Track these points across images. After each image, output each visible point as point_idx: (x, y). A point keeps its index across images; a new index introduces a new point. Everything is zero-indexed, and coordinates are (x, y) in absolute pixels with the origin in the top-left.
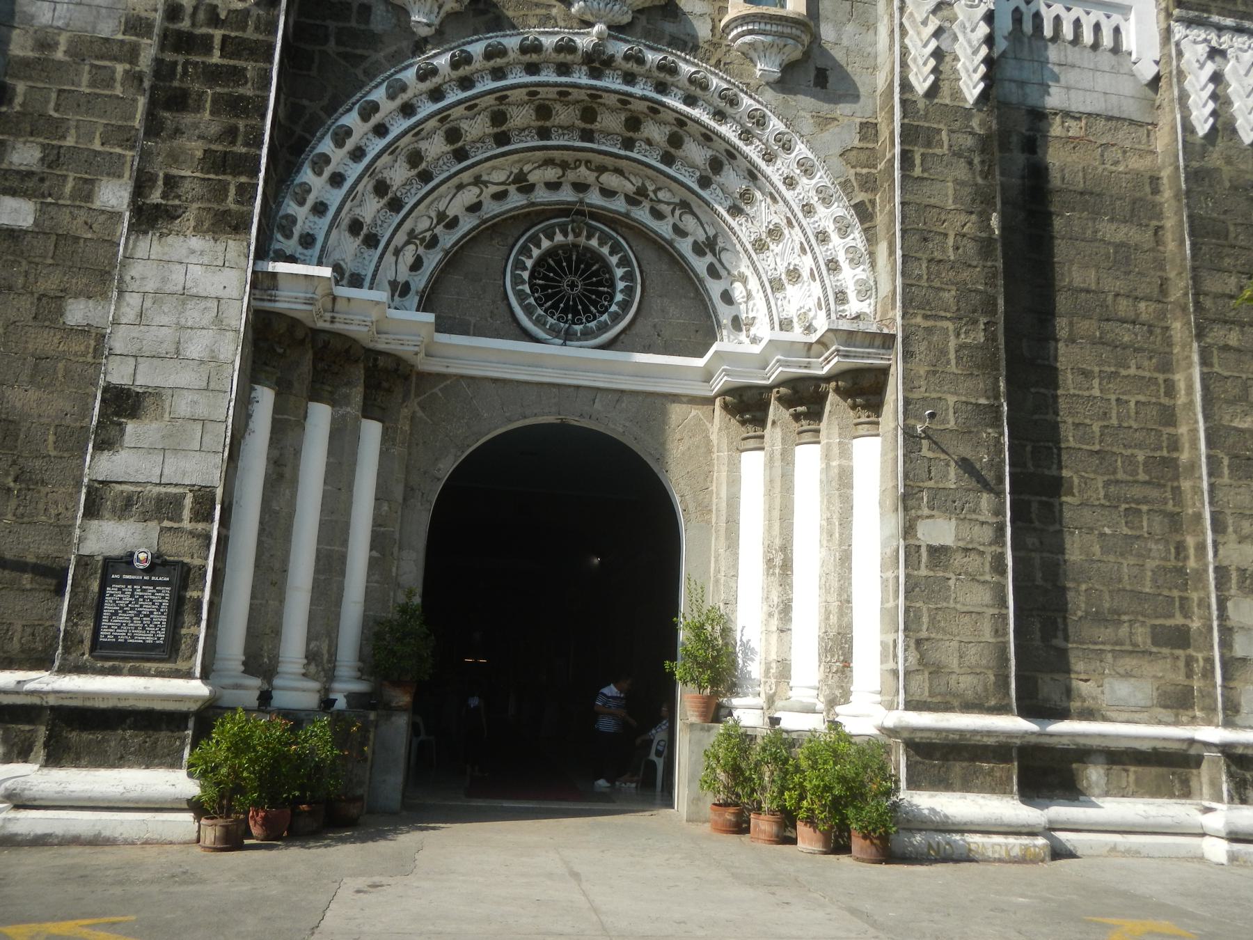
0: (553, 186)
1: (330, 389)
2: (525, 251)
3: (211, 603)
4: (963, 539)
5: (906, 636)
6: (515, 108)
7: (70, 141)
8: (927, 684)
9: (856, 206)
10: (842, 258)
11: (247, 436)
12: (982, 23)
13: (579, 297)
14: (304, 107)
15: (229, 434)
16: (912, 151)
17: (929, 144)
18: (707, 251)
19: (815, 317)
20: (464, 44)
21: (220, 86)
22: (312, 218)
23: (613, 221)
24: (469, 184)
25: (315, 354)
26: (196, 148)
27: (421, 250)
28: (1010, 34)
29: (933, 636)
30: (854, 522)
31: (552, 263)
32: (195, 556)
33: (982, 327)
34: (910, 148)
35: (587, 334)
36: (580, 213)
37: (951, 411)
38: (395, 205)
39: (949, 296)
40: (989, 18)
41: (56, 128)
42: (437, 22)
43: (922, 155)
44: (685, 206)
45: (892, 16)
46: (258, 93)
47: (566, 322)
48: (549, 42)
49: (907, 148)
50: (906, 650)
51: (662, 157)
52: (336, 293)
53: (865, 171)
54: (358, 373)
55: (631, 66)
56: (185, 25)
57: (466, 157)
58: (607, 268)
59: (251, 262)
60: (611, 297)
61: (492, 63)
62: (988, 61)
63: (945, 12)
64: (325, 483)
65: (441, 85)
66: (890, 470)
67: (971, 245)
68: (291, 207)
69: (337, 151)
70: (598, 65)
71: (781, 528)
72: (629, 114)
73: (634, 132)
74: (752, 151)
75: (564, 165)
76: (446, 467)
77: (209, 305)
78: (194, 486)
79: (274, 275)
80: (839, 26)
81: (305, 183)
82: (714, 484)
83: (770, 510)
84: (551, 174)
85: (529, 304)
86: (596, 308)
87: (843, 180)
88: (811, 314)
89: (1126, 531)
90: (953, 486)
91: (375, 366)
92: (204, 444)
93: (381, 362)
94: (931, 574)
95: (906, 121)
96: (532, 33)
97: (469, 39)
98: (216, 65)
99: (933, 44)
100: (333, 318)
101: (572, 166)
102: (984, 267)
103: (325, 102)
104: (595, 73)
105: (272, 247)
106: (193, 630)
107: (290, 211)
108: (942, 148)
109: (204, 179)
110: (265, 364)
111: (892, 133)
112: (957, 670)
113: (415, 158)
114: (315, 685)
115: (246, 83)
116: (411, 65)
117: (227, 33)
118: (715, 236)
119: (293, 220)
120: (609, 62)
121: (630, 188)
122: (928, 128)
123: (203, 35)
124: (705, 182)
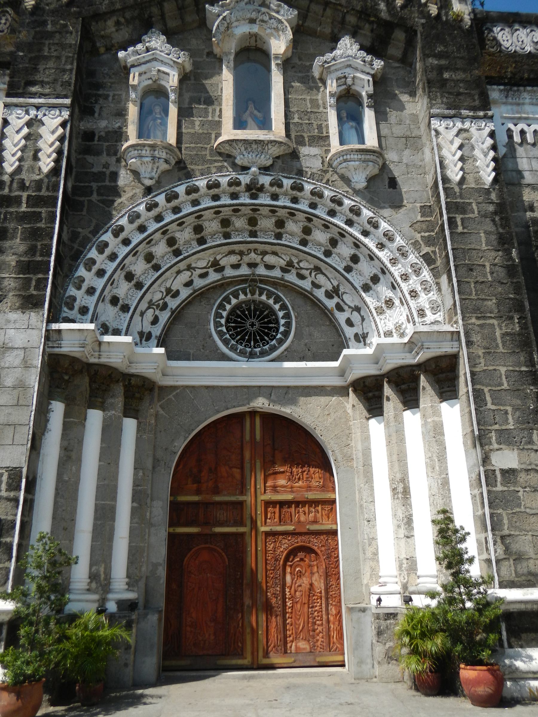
0: (236, 266)
1: (100, 400)
2: (221, 306)
3: (19, 545)
4: (525, 463)
5: (493, 535)
6: (207, 222)
8: (513, 568)
9: (423, 256)
10: (419, 288)
11: (46, 434)
12: (488, 138)
13: (257, 332)
14: (79, 233)
15: (31, 432)
16: (455, 218)
17: (464, 212)
18: (334, 295)
19: (406, 328)
20: (173, 187)
21: (26, 223)
22: (86, 297)
23: (275, 283)
24: (184, 270)
25: (91, 379)
26: (11, 259)
27: (157, 312)
28: (507, 144)
29: (512, 533)
30: (448, 458)
31: (239, 313)
32: (9, 513)
33: (517, 321)
34: (453, 215)
35: (263, 354)
36: (252, 280)
37: (504, 377)
38: (139, 286)
39: (491, 303)
40: (492, 135)
42: (156, 176)
43: (462, 219)
44: (317, 269)
45: (431, 141)
46: (49, 225)
47: (250, 347)
48: (224, 181)
49: (451, 216)
50: (494, 544)
51: (300, 242)
52: (101, 340)
53: (427, 234)
54: (119, 390)
55: (275, 189)
57: (180, 254)
58: (273, 312)
59: (45, 325)
60: (277, 330)
61: (190, 196)
62: (494, 159)
63: (465, 135)
64: (100, 460)
65: (161, 212)
66: (467, 420)
67: (500, 269)
68: (72, 291)
69: (100, 256)
70: (254, 191)
71: (400, 466)
72: (277, 219)
73: (281, 229)
75: (241, 253)
76: (180, 445)
77: (19, 353)
78: (8, 467)
79: (59, 331)
80: (400, 152)
81: (81, 276)
82: (353, 442)
83: (390, 455)
84: (234, 259)
85: (226, 338)
86: (268, 337)
87: (413, 241)
88: (404, 326)
90: (512, 427)
91: (130, 383)
92: (15, 440)
93: (133, 382)
94: (506, 489)
95: (449, 200)
96: (214, 177)
97: (176, 184)
98: (24, 212)
99: (459, 154)
100: (100, 355)
101: (246, 253)
102: (512, 283)
103: (92, 228)
104: (254, 196)
105: (61, 316)
106: (7, 564)
107: (72, 293)
108: (473, 213)
109: (16, 278)
110: (58, 387)
111: (441, 208)
112: (533, 556)
113: (149, 258)
114: (96, 597)
115: (41, 221)
116: (142, 202)
117: (30, 194)
118: (338, 286)
119: (74, 299)
120: (261, 189)
121: (283, 263)
122: (464, 203)
123: (16, 196)
124: (328, 254)
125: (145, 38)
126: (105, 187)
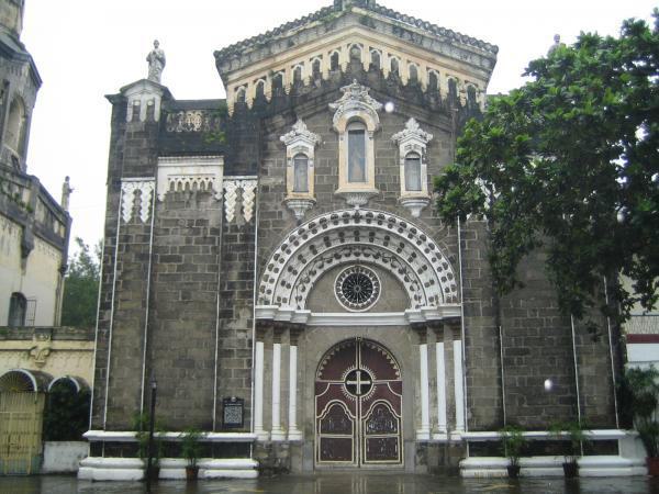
7: (199, 272)
23: (371, 264)
35: (363, 307)
41: (195, 268)
54: (288, 332)
56: (229, 233)
74: (413, 241)
75: (350, 249)
84: (347, 251)
89: (549, 365)
120: (361, 217)
125: (295, 126)
126: (278, 222)
